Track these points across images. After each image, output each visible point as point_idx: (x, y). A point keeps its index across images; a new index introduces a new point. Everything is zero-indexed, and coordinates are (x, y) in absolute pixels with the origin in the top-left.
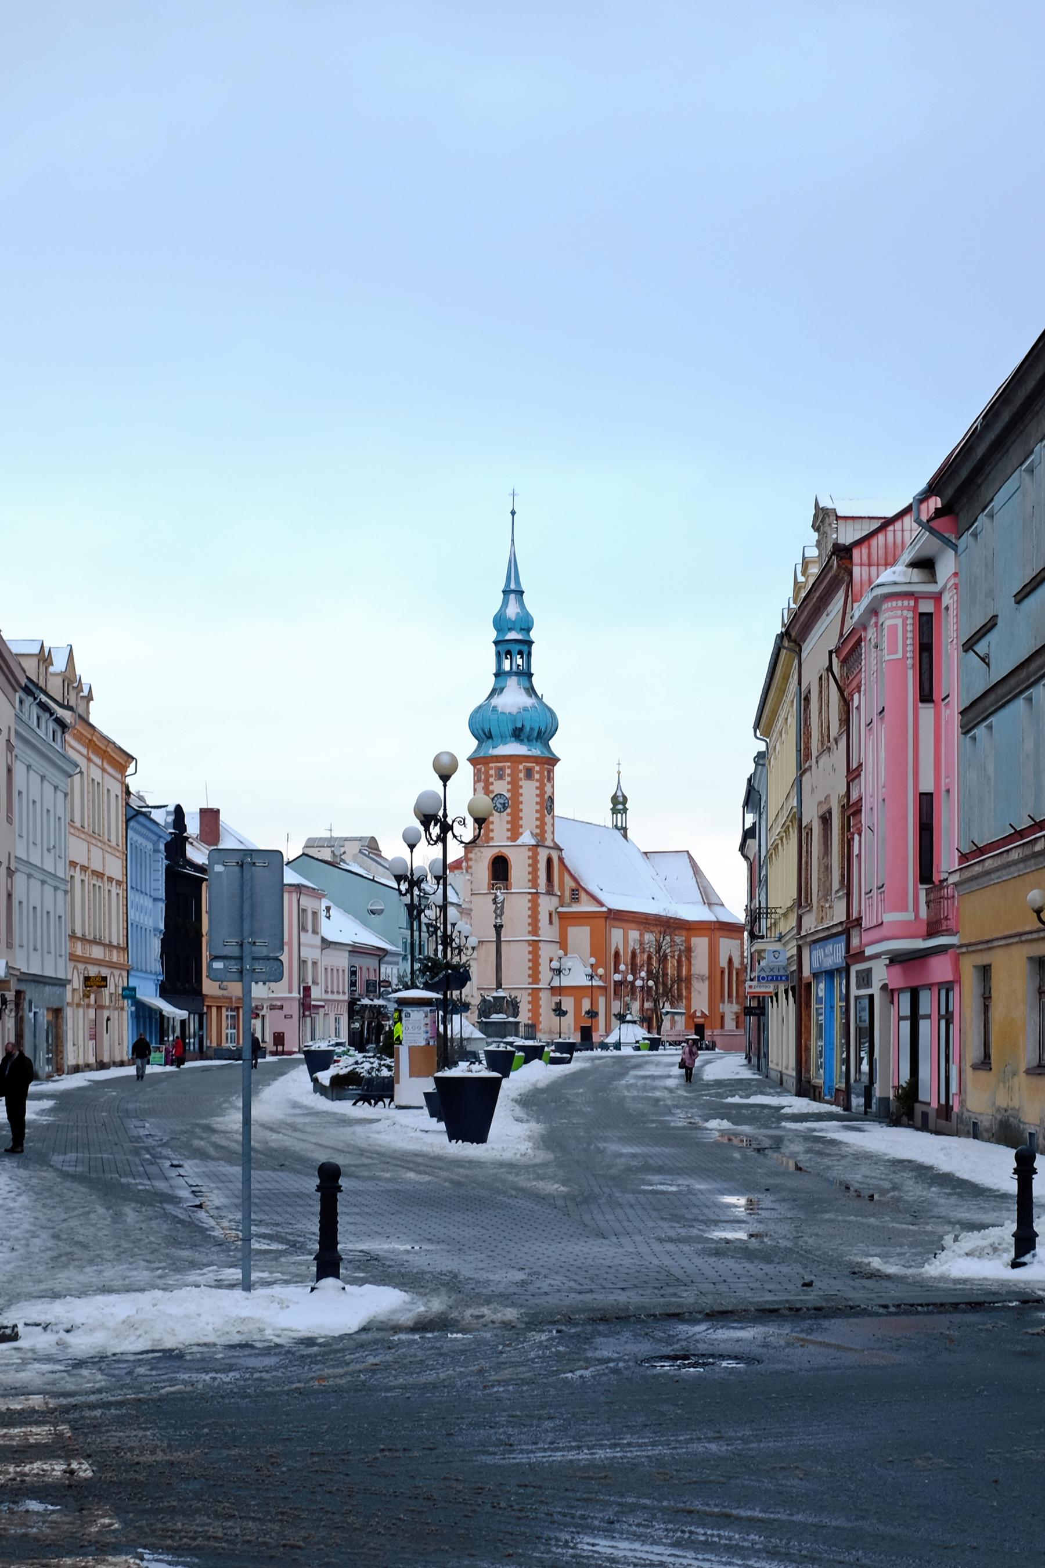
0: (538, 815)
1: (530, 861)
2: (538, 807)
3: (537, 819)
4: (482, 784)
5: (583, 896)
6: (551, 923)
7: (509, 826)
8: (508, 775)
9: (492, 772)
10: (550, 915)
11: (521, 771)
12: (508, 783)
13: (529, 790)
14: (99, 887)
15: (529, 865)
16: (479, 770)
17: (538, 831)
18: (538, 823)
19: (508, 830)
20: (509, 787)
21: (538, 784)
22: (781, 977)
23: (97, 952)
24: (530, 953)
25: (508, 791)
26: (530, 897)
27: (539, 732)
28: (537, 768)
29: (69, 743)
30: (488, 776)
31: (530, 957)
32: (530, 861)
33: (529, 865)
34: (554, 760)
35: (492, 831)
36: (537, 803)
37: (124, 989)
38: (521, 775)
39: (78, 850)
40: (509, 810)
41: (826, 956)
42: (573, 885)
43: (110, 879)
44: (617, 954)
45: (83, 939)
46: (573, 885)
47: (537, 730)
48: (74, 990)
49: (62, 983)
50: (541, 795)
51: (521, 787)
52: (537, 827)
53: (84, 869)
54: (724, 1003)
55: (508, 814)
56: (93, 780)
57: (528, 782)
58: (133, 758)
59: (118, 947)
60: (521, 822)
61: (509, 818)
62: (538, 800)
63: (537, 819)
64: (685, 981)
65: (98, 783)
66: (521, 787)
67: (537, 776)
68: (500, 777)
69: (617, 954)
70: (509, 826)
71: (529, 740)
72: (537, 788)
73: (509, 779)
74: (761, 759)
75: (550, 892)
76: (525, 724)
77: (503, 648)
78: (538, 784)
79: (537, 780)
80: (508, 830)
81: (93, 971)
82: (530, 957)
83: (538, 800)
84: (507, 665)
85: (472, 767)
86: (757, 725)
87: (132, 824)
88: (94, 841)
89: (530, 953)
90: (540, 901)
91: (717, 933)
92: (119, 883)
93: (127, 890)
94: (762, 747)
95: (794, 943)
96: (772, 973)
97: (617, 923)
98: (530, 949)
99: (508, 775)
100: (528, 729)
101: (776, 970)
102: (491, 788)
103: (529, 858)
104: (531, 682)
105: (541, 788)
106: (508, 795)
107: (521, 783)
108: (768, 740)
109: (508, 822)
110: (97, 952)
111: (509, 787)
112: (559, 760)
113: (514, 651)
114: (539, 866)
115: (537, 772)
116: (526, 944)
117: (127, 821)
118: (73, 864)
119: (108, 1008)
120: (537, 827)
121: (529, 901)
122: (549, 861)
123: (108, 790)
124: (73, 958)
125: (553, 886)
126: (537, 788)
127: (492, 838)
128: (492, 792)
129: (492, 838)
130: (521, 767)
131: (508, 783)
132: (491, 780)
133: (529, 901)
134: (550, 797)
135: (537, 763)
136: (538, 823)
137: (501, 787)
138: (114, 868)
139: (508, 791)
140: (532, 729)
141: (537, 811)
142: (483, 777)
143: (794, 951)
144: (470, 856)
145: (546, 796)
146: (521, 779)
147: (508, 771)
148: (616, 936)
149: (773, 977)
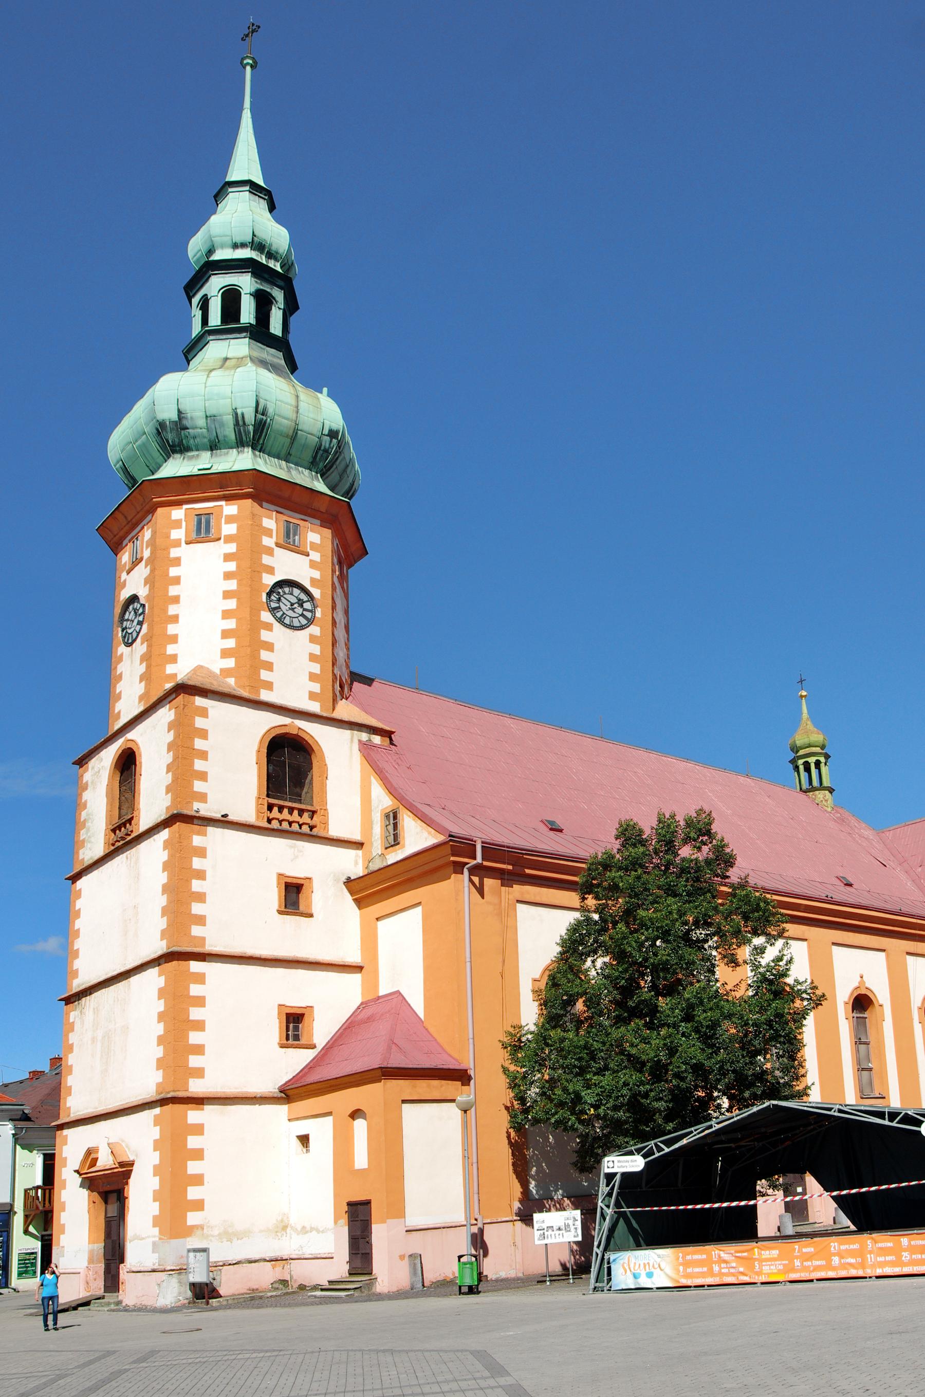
5: (409, 823)
11: (177, 524)
17: (230, 663)
21: (232, 548)
28: (230, 509)
47: (229, 420)
51: (177, 562)
66: (177, 562)
71: (214, 446)
72: (228, 557)
78: (232, 548)
79: (229, 539)
100: (202, 422)
115: (230, 519)
120: (225, 653)
126: (228, 557)
146: (177, 543)
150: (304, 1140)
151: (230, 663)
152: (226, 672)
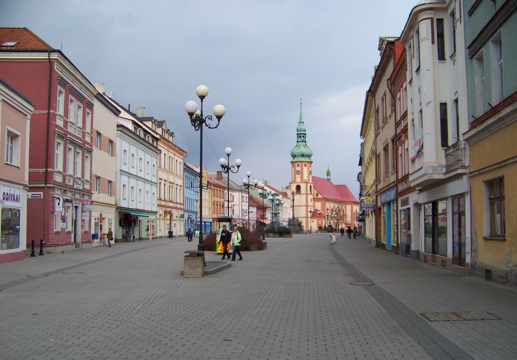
0: (308, 175)
1: (306, 186)
2: (308, 173)
3: (308, 176)
4: (293, 168)
6: (311, 201)
7: (301, 178)
8: (300, 166)
9: (296, 165)
10: (311, 199)
11: (303, 165)
12: (300, 168)
13: (305, 169)
14: (172, 187)
15: (306, 187)
16: (293, 165)
17: (308, 179)
18: (308, 177)
19: (300, 179)
20: (301, 168)
21: (308, 168)
22: (370, 207)
23: (170, 204)
24: (306, 209)
25: (300, 169)
26: (306, 195)
27: (308, 155)
28: (307, 164)
29: (159, 144)
30: (295, 166)
31: (306, 210)
32: (306, 186)
33: (306, 187)
34: (311, 162)
35: (296, 179)
36: (307, 172)
37: (181, 215)
38: (304, 166)
39: (163, 175)
40: (300, 174)
41: (387, 197)
42: (317, 192)
43: (177, 185)
44: (328, 209)
45: (165, 200)
46: (317, 192)
48: (160, 215)
49: (155, 213)
50: (309, 170)
51: (303, 169)
52: (307, 178)
53: (165, 181)
54: (355, 221)
55: (300, 175)
56: (170, 157)
57: (305, 167)
58: (186, 153)
59: (180, 204)
60: (303, 177)
61: (301, 176)
62: (308, 172)
63: (308, 176)
64: (345, 215)
65: (172, 158)
66: (303, 169)
67: (307, 166)
68: (298, 166)
69: (328, 209)
70: (301, 178)
71: (305, 157)
72: (307, 169)
73: (300, 167)
74: (362, 145)
75: (311, 194)
76: (304, 153)
77: (299, 135)
78: (308, 168)
79: (307, 167)
80: (300, 179)
81: (169, 210)
82: (306, 210)
83: (308, 172)
84: (300, 139)
85: (291, 164)
86: (361, 135)
87: (185, 170)
88: (170, 174)
89: (306, 209)
90: (308, 196)
91: (353, 204)
92: (181, 186)
93: (184, 188)
94: (363, 141)
95: (375, 195)
96: (367, 206)
97: (327, 202)
98: (306, 208)
99: (300, 166)
100: (305, 155)
101: (368, 205)
102: (296, 169)
103: (306, 186)
104: (306, 143)
105: (309, 169)
106: (300, 170)
107: (303, 167)
108: (365, 139)
109: (300, 177)
110: (170, 204)
111: (301, 168)
112: (313, 162)
113: (302, 136)
114: (308, 187)
115: (308, 165)
116: (305, 207)
117: (184, 170)
118: (161, 179)
119: (175, 220)
120: (307, 178)
121: (306, 196)
122: (311, 186)
123: (177, 160)
124: (159, 205)
125: (311, 192)
126: (307, 169)
127: (296, 181)
128: (296, 170)
129: (296, 181)
130: (303, 164)
131: (300, 168)
132: (296, 167)
133: (306, 196)
134: (311, 171)
135: (307, 163)
136: (308, 177)
137: (298, 169)
138: (180, 182)
139: (300, 169)
140: (306, 155)
141: (307, 174)
142: (294, 166)
143: (375, 198)
144: (291, 185)
145: (310, 171)
147: (300, 165)
148: (328, 205)
149: (367, 207)
150: (313, 221)
151: (308, 179)
152: (308, 180)
